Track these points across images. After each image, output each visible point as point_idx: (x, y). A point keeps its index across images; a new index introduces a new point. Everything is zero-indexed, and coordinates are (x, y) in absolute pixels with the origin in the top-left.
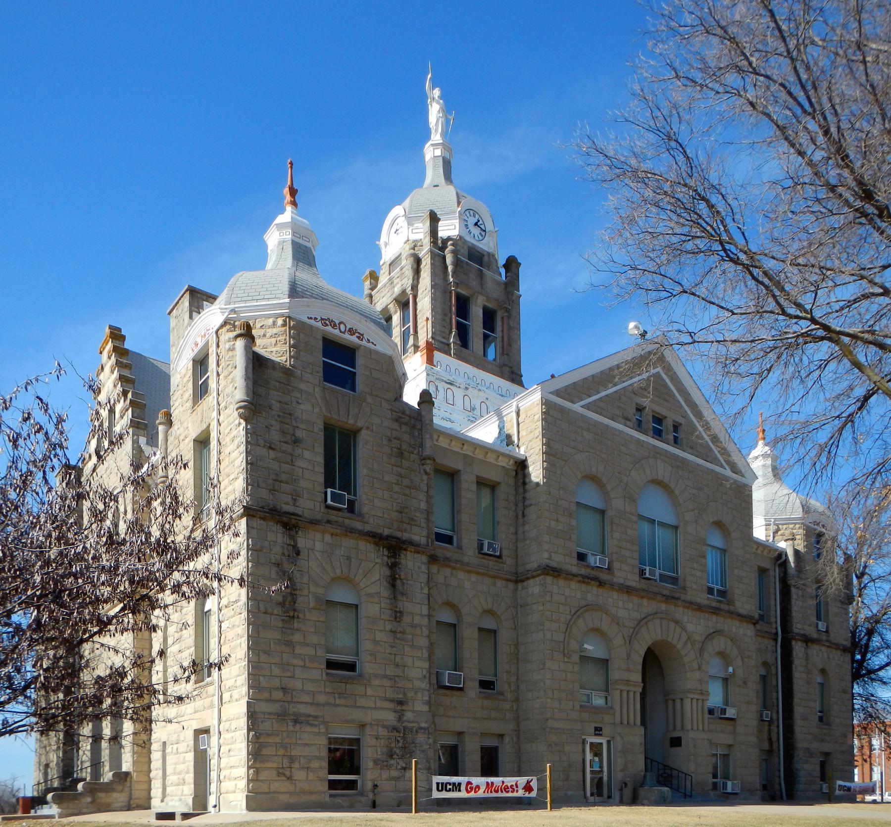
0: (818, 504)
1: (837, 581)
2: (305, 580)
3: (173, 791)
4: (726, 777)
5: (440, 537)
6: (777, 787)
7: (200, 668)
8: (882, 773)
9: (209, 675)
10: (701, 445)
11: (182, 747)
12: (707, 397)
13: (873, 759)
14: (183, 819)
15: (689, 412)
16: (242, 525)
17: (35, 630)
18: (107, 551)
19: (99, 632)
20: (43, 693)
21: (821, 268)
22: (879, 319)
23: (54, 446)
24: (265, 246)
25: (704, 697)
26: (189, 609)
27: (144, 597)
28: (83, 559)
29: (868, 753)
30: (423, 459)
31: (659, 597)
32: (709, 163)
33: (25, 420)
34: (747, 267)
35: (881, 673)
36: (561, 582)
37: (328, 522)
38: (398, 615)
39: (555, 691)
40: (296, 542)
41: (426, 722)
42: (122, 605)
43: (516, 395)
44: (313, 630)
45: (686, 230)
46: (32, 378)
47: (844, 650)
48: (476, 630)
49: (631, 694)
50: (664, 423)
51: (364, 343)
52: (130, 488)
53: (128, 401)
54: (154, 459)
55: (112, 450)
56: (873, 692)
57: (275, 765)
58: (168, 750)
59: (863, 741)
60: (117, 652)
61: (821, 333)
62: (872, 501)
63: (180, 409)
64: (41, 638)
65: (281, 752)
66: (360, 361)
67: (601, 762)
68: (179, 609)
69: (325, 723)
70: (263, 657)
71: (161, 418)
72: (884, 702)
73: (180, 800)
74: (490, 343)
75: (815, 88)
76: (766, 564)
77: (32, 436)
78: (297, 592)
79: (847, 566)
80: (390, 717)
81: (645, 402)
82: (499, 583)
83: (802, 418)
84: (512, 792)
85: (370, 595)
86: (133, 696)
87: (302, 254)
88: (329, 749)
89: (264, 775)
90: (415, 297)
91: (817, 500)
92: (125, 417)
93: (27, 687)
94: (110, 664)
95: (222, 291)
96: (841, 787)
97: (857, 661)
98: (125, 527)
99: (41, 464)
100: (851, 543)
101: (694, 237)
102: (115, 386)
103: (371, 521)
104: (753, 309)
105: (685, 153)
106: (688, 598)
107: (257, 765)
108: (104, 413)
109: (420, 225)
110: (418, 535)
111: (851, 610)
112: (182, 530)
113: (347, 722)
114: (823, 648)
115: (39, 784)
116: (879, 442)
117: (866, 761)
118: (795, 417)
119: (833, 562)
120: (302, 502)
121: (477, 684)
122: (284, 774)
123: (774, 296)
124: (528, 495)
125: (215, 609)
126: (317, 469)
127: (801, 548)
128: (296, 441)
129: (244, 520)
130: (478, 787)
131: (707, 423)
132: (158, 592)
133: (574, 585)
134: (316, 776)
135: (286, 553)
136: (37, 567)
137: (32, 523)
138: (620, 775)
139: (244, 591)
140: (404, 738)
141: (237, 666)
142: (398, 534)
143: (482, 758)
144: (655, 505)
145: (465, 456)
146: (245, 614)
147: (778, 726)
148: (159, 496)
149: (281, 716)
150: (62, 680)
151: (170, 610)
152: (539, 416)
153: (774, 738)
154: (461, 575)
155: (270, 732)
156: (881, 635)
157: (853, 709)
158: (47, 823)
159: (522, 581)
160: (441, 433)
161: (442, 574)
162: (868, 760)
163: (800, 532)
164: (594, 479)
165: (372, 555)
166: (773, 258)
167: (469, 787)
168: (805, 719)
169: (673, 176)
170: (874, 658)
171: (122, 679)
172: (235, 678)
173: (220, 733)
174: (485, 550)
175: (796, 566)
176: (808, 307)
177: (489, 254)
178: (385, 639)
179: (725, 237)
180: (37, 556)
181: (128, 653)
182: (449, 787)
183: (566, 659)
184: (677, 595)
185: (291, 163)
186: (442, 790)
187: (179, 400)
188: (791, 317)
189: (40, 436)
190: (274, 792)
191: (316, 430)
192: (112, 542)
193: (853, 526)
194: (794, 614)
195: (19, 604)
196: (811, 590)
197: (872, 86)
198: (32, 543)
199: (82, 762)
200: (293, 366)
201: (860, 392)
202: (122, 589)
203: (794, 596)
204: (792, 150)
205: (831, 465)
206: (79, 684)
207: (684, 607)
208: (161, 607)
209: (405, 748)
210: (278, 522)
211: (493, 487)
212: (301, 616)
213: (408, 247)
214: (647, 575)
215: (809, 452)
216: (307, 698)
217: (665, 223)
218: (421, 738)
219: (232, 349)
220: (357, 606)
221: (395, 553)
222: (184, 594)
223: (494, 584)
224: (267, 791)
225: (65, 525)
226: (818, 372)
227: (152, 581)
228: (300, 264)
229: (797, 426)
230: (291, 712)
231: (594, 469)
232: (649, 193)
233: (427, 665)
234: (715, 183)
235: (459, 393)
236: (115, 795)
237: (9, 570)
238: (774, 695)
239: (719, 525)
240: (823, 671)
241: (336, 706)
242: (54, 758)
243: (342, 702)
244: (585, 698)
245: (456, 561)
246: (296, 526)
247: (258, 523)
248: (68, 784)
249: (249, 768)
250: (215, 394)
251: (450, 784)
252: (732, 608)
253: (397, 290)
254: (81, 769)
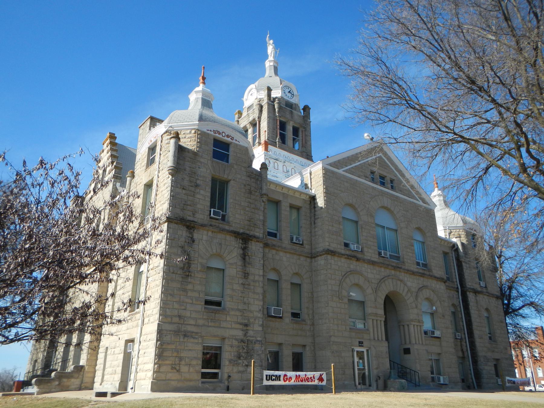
0: (471, 219)
1: (487, 259)
2: (196, 255)
3: (107, 379)
4: (439, 374)
5: (270, 234)
6: (471, 380)
7: (133, 304)
8: (532, 372)
9: (138, 308)
10: (406, 190)
11: (117, 350)
12: (406, 167)
13: (525, 363)
14: (112, 397)
15: (398, 174)
16: (165, 227)
17: (44, 281)
18: (91, 239)
19: (80, 283)
20: (42, 317)
21: (455, 111)
22: (488, 133)
23: (72, 187)
24: (189, 100)
25: (421, 324)
26: (131, 271)
27: (107, 264)
28: (78, 243)
29: (521, 359)
30: (262, 195)
31: (390, 267)
32: (397, 69)
33: (60, 174)
34: (420, 111)
35: (521, 311)
36: (336, 258)
37: (211, 225)
38: (246, 275)
39: (335, 320)
40: (193, 235)
41: (260, 337)
42: (95, 268)
43: (309, 165)
44: (199, 282)
45: (389, 95)
46: (67, 155)
47: (497, 298)
48: (290, 284)
49: (379, 322)
50: (386, 179)
51: (234, 141)
52: (108, 207)
53: (113, 166)
54: (122, 194)
55: (102, 189)
56: (518, 323)
57: (170, 362)
58: (109, 352)
59: (518, 352)
60: (88, 293)
61: (459, 139)
62: (499, 218)
63: (140, 170)
64: (47, 285)
65: (175, 354)
66: (231, 149)
67: (364, 363)
68: (125, 270)
69: (202, 337)
70: (169, 298)
71: (129, 174)
72: (525, 328)
73: (112, 384)
74: (296, 142)
75: (442, 42)
76: (447, 250)
77: (62, 182)
78: (192, 262)
79: (491, 252)
80: (239, 334)
81: (375, 169)
82: (302, 258)
83: (456, 177)
84: (311, 381)
85: (231, 264)
86: (93, 319)
87: (206, 103)
88: (203, 353)
89: (163, 369)
90: (260, 122)
91: (470, 217)
92: (111, 174)
93: (34, 313)
94: (82, 300)
95: (166, 118)
96: (509, 381)
97: (506, 304)
98: (103, 227)
99: (64, 195)
100: (491, 239)
101: (393, 98)
102: (108, 159)
103: (234, 225)
104: (425, 128)
105: (385, 65)
106: (406, 268)
107: (160, 362)
108: (101, 172)
109: (263, 92)
110: (259, 233)
111: (498, 275)
112: (133, 229)
113: (215, 336)
114: (485, 297)
115: (29, 372)
116: (497, 189)
117: (521, 364)
118: (452, 177)
119: (483, 249)
120: (197, 215)
121: (290, 315)
122: (175, 369)
123: (434, 123)
124: (317, 213)
125: (145, 271)
126: (206, 199)
127: (464, 241)
128: (197, 186)
129: (166, 224)
130: (291, 378)
131: (408, 179)
132: (115, 261)
133: (343, 260)
134: (194, 369)
135: (187, 241)
136: (52, 247)
137: (54, 224)
138: (375, 372)
139: (162, 261)
140: (247, 347)
141: (155, 302)
142: (248, 232)
143: (293, 359)
144: (384, 219)
145: (284, 194)
146: (162, 273)
147: (466, 342)
148: (123, 211)
149: (177, 332)
150: (54, 310)
151: (121, 271)
152: (321, 175)
153: (465, 350)
154: (281, 254)
155: (169, 342)
156: (516, 289)
157: (508, 333)
158: (29, 397)
159: (315, 257)
160: (271, 182)
161: (270, 253)
162: (522, 363)
163: (463, 234)
164: (351, 206)
165: (233, 243)
166: (432, 107)
167: (286, 378)
168: (481, 338)
169: (381, 74)
170: (515, 303)
171: (88, 309)
172: (152, 311)
173: (140, 342)
174: (294, 241)
175: (463, 251)
176: (452, 128)
177: (295, 104)
178: (239, 288)
179: (407, 98)
180: (53, 241)
181: (94, 295)
182: (273, 378)
183: (340, 301)
184: (400, 266)
185: (204, 67)
186: (269, 380)
187: (140, 166)
188: (444, 132)
189: (66, 182)
190: (169, 380)
191: (207, 180)
192: (95, 234)
193: (491, 230)
194: (466, 277)
195: (38, 267)
196: (473, 264)
197: (467, 41)
198: (52, 234)
199: (57, 359)
200: (198, 151)
201: (483, 166)
202: (96, 259)
203: (465, 267)
204: (435, 65)
205: (474, 200)
206: (63, 312)
207: (404, 273)
208: (116, 269)
209: (248, 353)
210: (184, 225)
211: (298, 209)
212: (192, 275)
213: (257, 101)
214: (383, 255)
215: (463, 195)
216: (192, 322)
217: (379, 92)
218: (257, 347)
219: (168, 143)
220: (224, 270)
221: (246, 242)
222: (129, 262)
223: (299, 259)
224: (164, 379)
225: (71, 225)
226: (460, 157)
227: (113, 255)
228: (205, 107)
229: (454, 181)
230: (182, 330)
231: (351, 201)
232: (370, 80)
233: (261, 303)
234: (401, 77)
235: (281, 165)
236: (73, 380)
237: (37, 249)
238: (461, 323)
239: (419, 229)
240: (487, 310)
241: (208, 326)
242: (41, 356)
243: (212, 324)
244: (352, 324)
245: (279, 247)
246: (193, 227)
247: (173, 225)
248: (46, 373)
249: (155, 364)
250: (158, 163)
251: (274, 376)
252: (431, 274)
253: (251, 119)
254: (56, 364)
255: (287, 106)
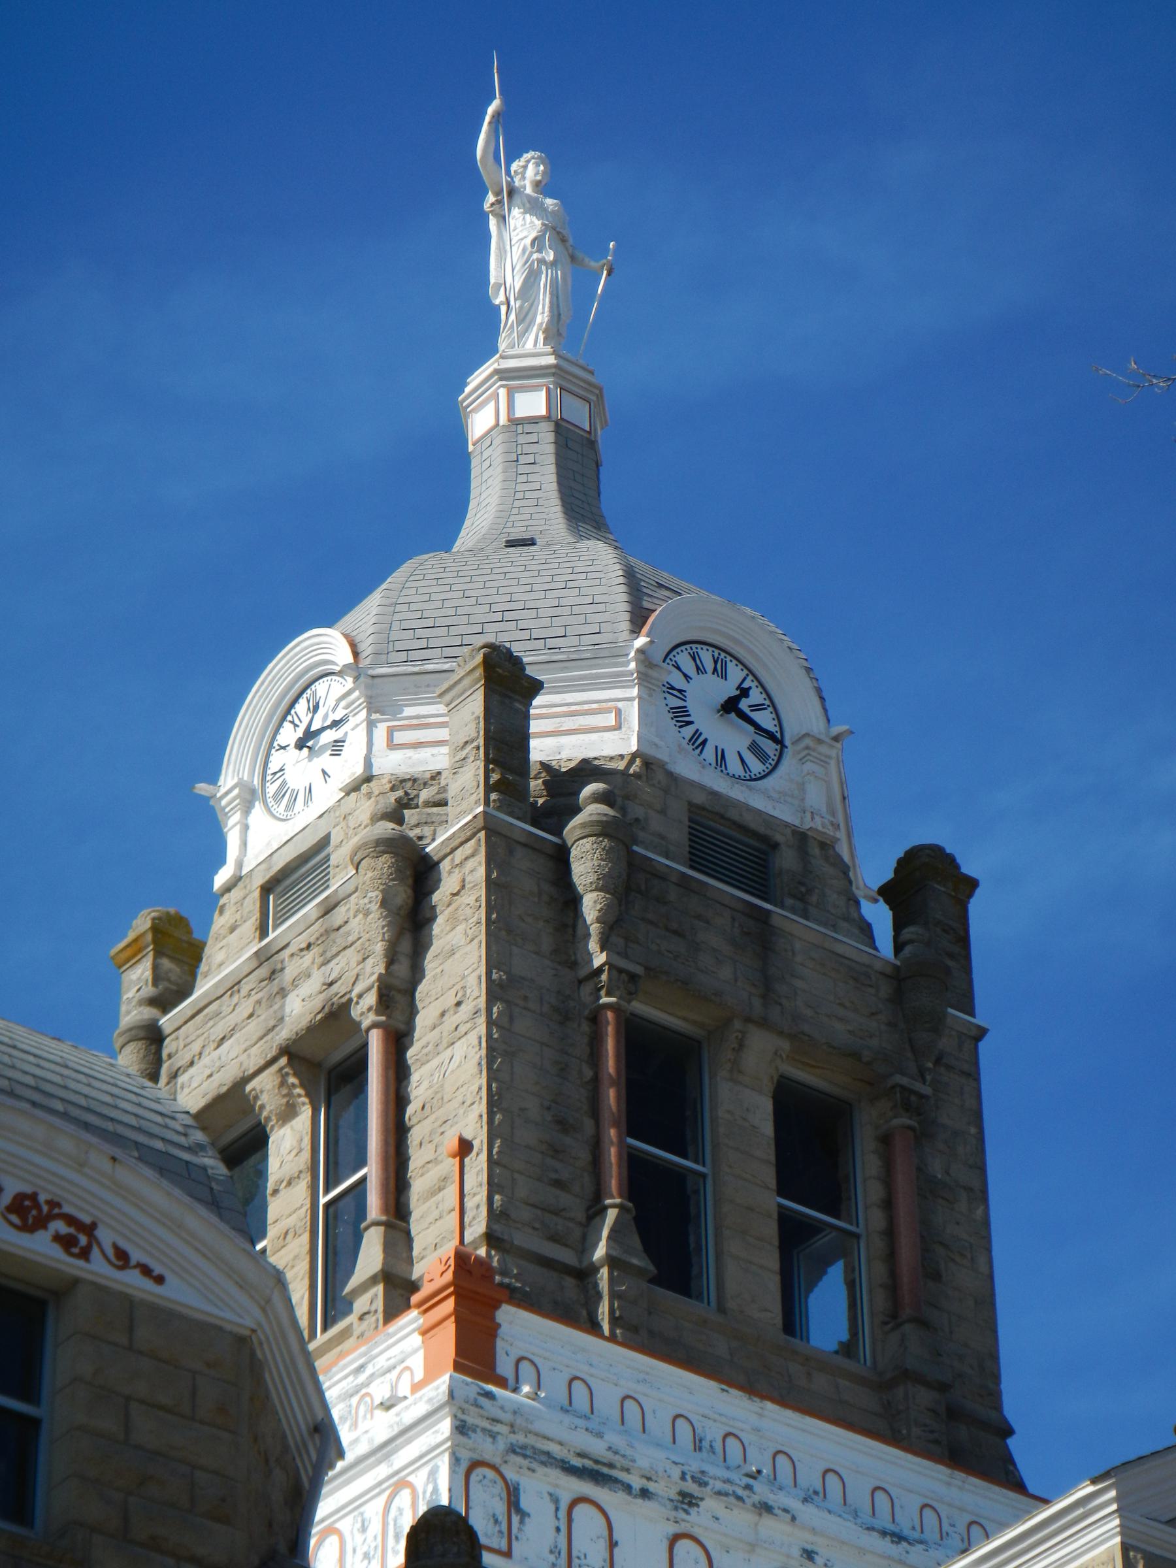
51: (98, 1268)
66: (66, 1360)
90: (399, 1041)
177: (802, 838)
213: (364, 808)
253: (300, 1008)
255: (701, 860)
